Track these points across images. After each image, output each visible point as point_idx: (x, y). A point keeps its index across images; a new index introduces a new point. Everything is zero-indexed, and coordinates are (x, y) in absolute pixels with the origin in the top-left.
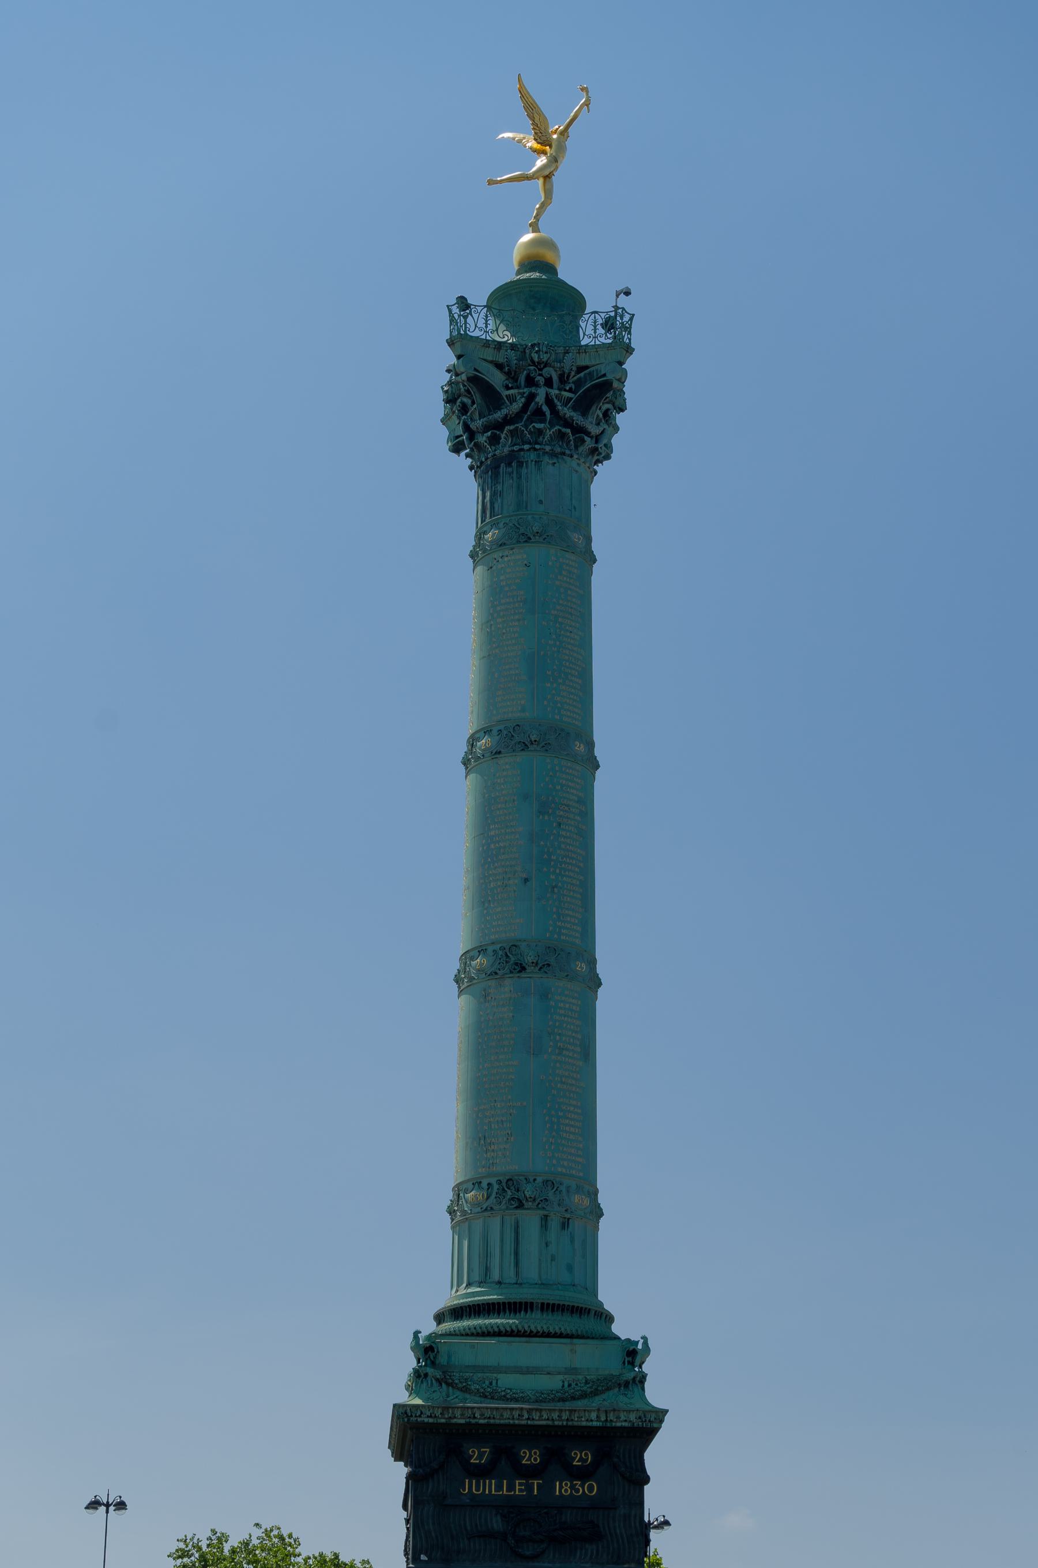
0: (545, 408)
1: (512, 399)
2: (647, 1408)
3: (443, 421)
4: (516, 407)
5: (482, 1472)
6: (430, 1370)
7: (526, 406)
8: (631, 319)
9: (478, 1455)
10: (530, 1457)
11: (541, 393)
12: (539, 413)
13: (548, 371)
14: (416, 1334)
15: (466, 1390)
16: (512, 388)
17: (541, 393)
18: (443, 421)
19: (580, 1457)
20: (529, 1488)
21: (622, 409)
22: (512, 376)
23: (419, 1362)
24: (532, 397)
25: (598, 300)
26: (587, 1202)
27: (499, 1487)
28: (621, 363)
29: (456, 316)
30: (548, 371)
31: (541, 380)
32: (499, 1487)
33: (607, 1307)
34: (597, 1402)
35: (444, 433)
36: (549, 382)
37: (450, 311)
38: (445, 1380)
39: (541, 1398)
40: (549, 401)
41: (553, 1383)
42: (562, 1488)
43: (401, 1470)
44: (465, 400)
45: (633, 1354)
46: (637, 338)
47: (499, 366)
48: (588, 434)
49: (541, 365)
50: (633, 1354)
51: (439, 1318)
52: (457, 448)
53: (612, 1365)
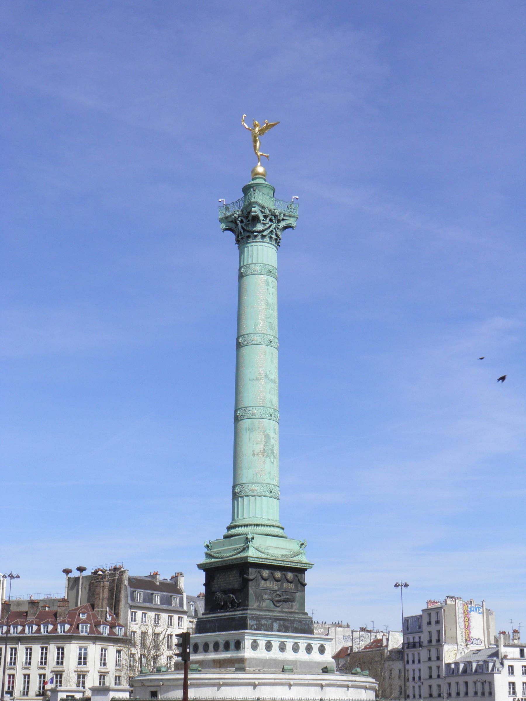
5: (265, 580)
9: (266, 573)
10: (278, 575)
15: (262, 553)
19: (290, 575)
20: (278, 584)
22: (265, 217)
24: (271, 226)
27: (270, 584)
32: (270, 584)
39: (282, 556)
40: (275, 229)
41: (284, 553)
42: (286, 585)
47: (262, 212)
49: (275, 216)
53: (294, 546)
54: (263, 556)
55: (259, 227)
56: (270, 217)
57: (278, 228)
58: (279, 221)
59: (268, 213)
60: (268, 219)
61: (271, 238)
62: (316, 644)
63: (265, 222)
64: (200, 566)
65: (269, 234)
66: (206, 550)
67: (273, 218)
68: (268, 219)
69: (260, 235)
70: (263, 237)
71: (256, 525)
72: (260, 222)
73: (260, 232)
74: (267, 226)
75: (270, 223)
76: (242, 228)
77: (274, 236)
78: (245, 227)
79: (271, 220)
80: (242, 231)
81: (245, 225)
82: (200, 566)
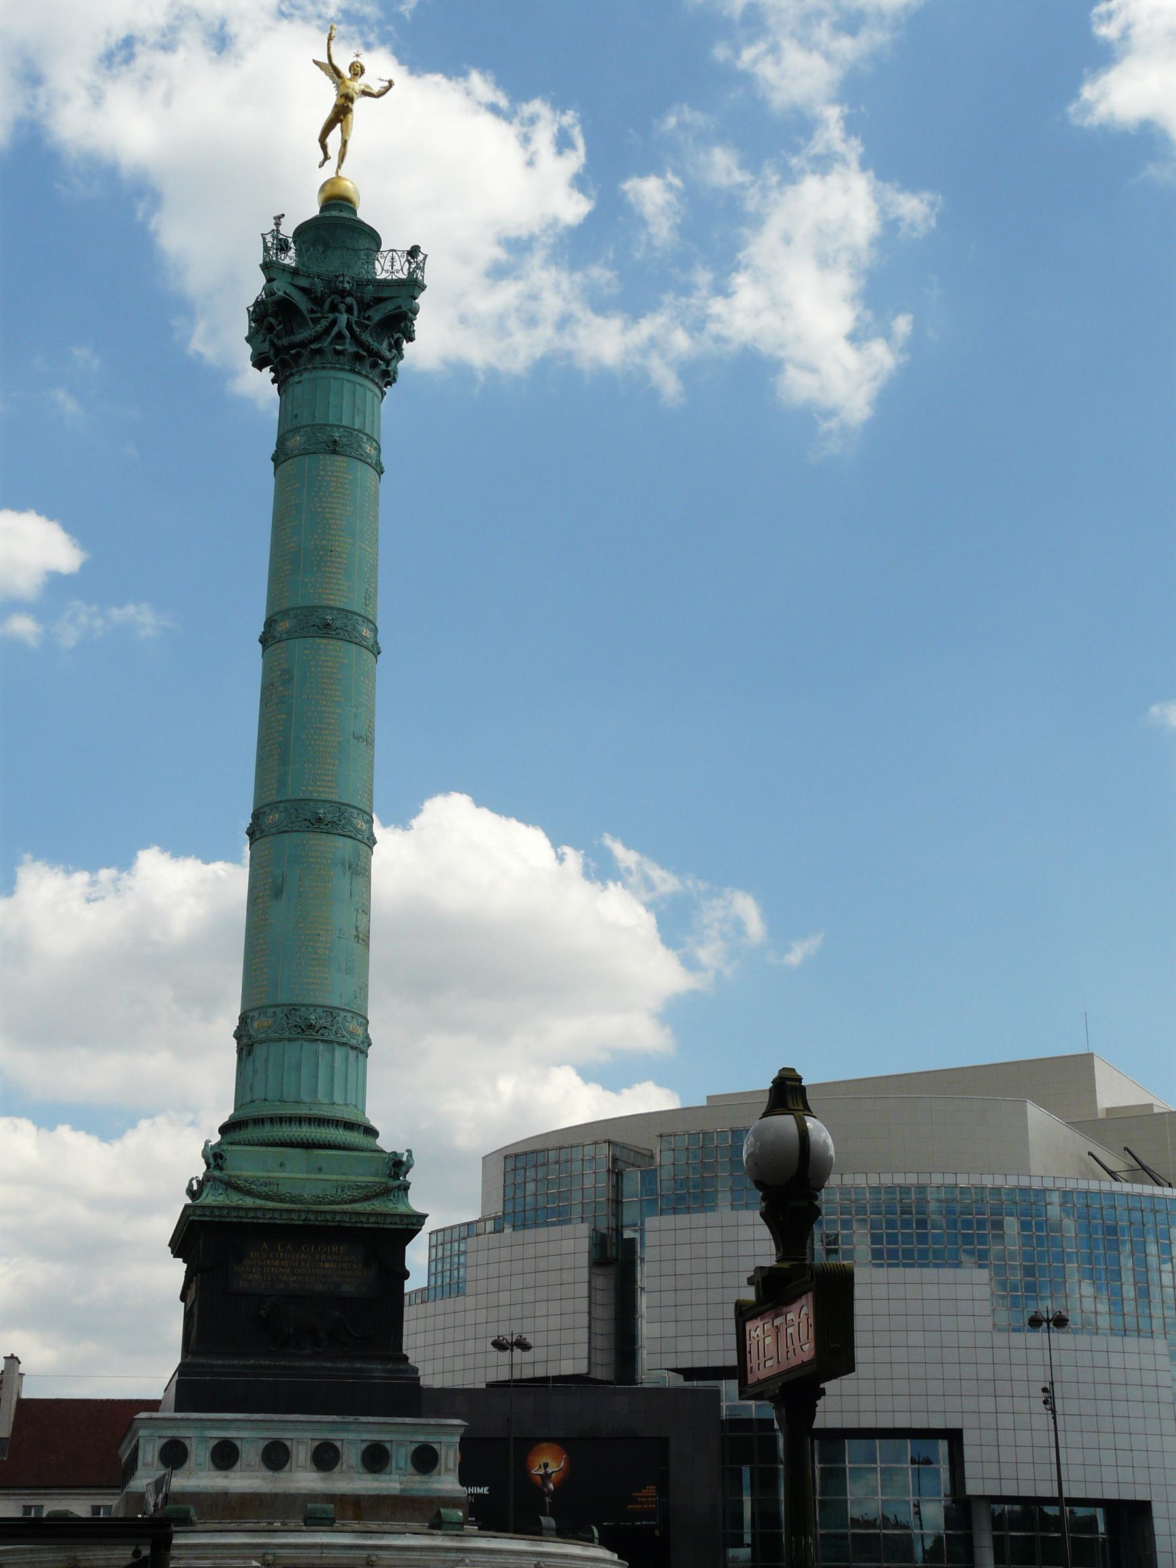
1: (316, 321)
2: (410, 1212)
3: (248, 340)
4: (319, 328)
6: (217, 1173)
7: (327, 331)
8: (425, 259)
11: (343, 318)
12: (340, 336)
13: (349, 300)
14: (207, 1143)
15: (249, 1193)
16: (316, 312)
17: (343, 318)
18: (248, 340)
21: (411, 339)
22: (317, 301)
23: (208, 1168)
24: (334, 322)
25: (394, 239)
26: (360, 1031)
28: (415, 298)
29: (269, 245)
30: (349, 300)
31: (342, 307)
33: (374, 1123)
34: (366, 1207)
35: (248, 350)
36: (349, 310)
37: (264, 239)
38: (231, 1185)
39: (319, 1201)
40: (349, 326)
43: (703, 1102)
44: (272, 320)
45: (398, 1166)
46: (429, 277)
47: (304, 290)
48: (383, 359)
49: (343, 294)
50: (398, 1166)
51: (224, 1130)
54: (249, 1202)
56: (328, 301)
57: (367, 326)
58: (364, 306)
59: (319, 286)
60: (327, 306)
62: (401, 1444)
63: (319, 315)
65: (333, 342)
67: (337, 299)
68: (327, 306)
71: (259, 1121)
73: (303, 344)
74: (324, 323)
75: (331, 316)
76: (272, 344)
77: (350, 347)
78: (275, 341)
79: (334, 308)
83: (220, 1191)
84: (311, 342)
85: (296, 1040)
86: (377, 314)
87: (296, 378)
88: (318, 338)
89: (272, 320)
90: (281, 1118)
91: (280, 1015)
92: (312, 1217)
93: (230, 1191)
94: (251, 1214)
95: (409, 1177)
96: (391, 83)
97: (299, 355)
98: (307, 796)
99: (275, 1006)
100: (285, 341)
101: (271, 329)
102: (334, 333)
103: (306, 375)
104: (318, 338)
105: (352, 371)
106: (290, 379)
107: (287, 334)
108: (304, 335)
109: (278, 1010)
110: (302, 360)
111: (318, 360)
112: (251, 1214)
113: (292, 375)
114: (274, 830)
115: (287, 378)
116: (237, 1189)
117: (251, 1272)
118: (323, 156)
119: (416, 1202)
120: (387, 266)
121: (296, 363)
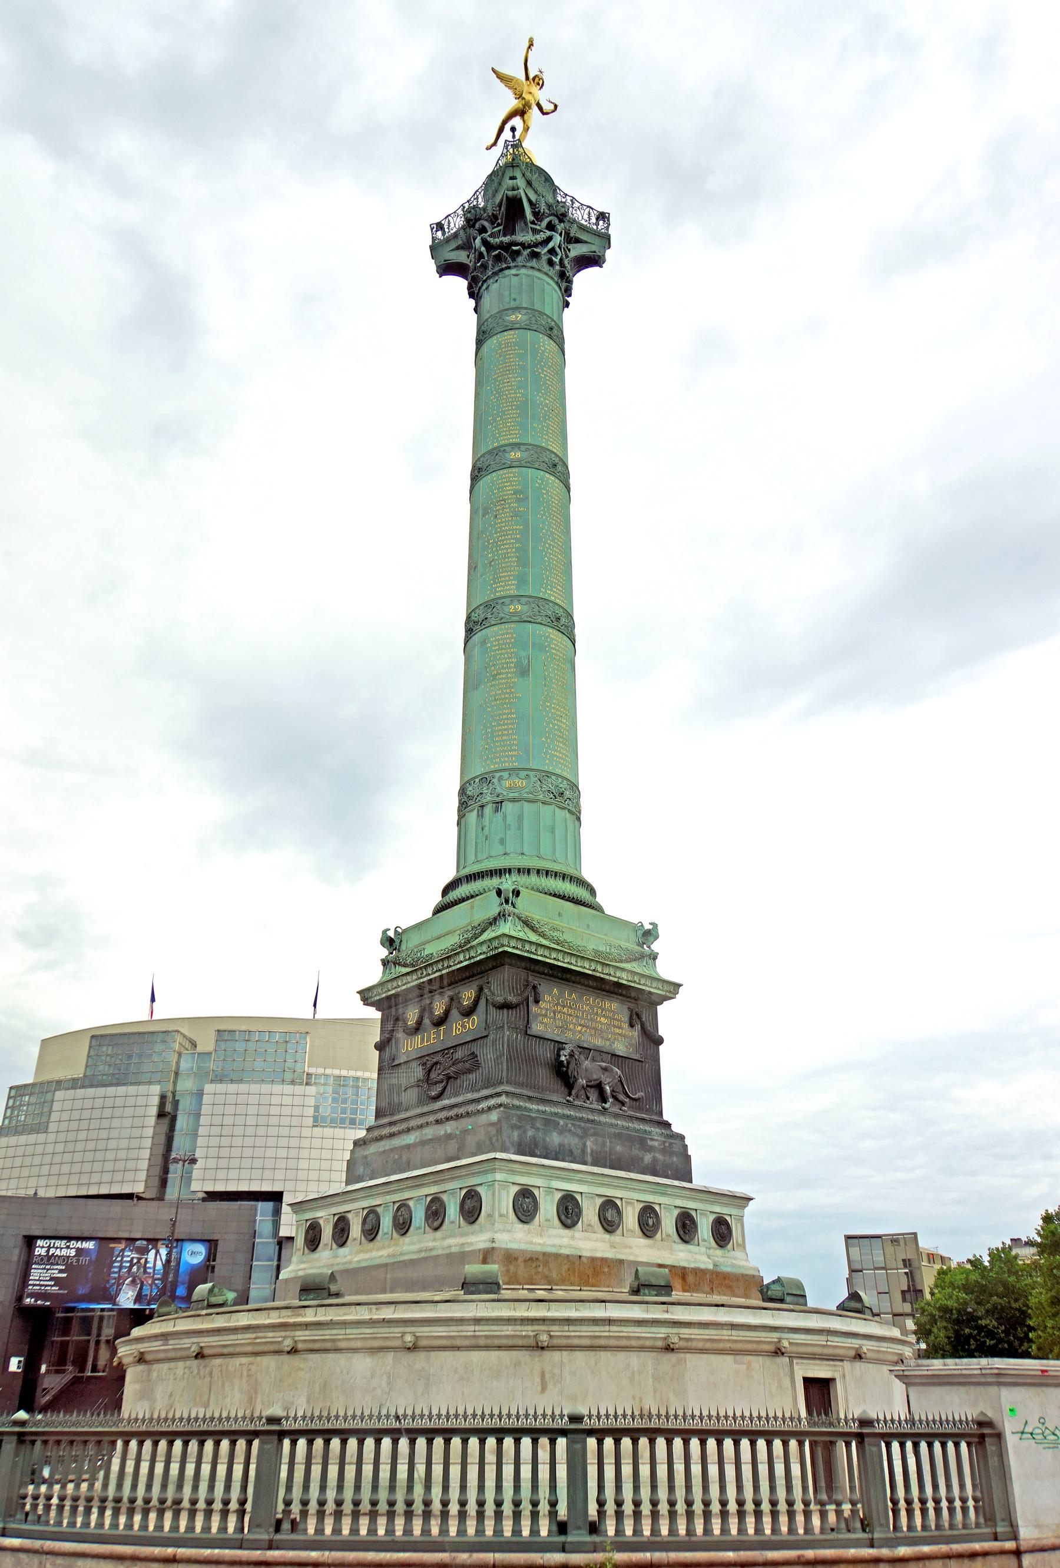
0: (558, 249)
15: (543, 935)
22: (536, 214)
24: (549, 239)
38: (527, 923)
44: (486, 224)
52: (446, 269)
55: (524, 236)
61: (551, 263)
63: (538, 227)
64: (366, 996)
66: (384, 953)
69: (526, 252)
70: (535, 255)
72: (526, 223)
73: (523, 246)
74: (541, 237)
75: (549, 233)
76: (485, 242)
79: (551, 227)
80: (483, 249)
81: (491, 236)
82: (366, 996)
83: (519, 928)
84: (530, 246)
85: (550, 804)
86: (576, 250)
87: (514, 271)
88: (536, 245)
89: (486, 224)
90: (547, 872)
91: (533, 779)
92: (599, 969)
93: (526, 929)
94: (554, 955)
95: (656, 947)
96: (556, 106)
97: (518, 253)
98: (546, 597)
99: (527, 769)
100: (506, 239)
101: (483, 230)
102: (551, 245)
103: (523, 271)
104: (536, 245)
105: (557, 283)
106: (507, 272)
107: (505, 235)
108: (528, 238)
109: (531, 773)
110: (520, 259)
111: (534, 263)
112: (554, 955)
113: (509, 268)
114: (517, 619)
115: (502, 270)
116: (533, 929)
117: (545, 1015)
118: (493, 141)
119: (665, 969)
120: (586, 217)
121: (514, 260)
